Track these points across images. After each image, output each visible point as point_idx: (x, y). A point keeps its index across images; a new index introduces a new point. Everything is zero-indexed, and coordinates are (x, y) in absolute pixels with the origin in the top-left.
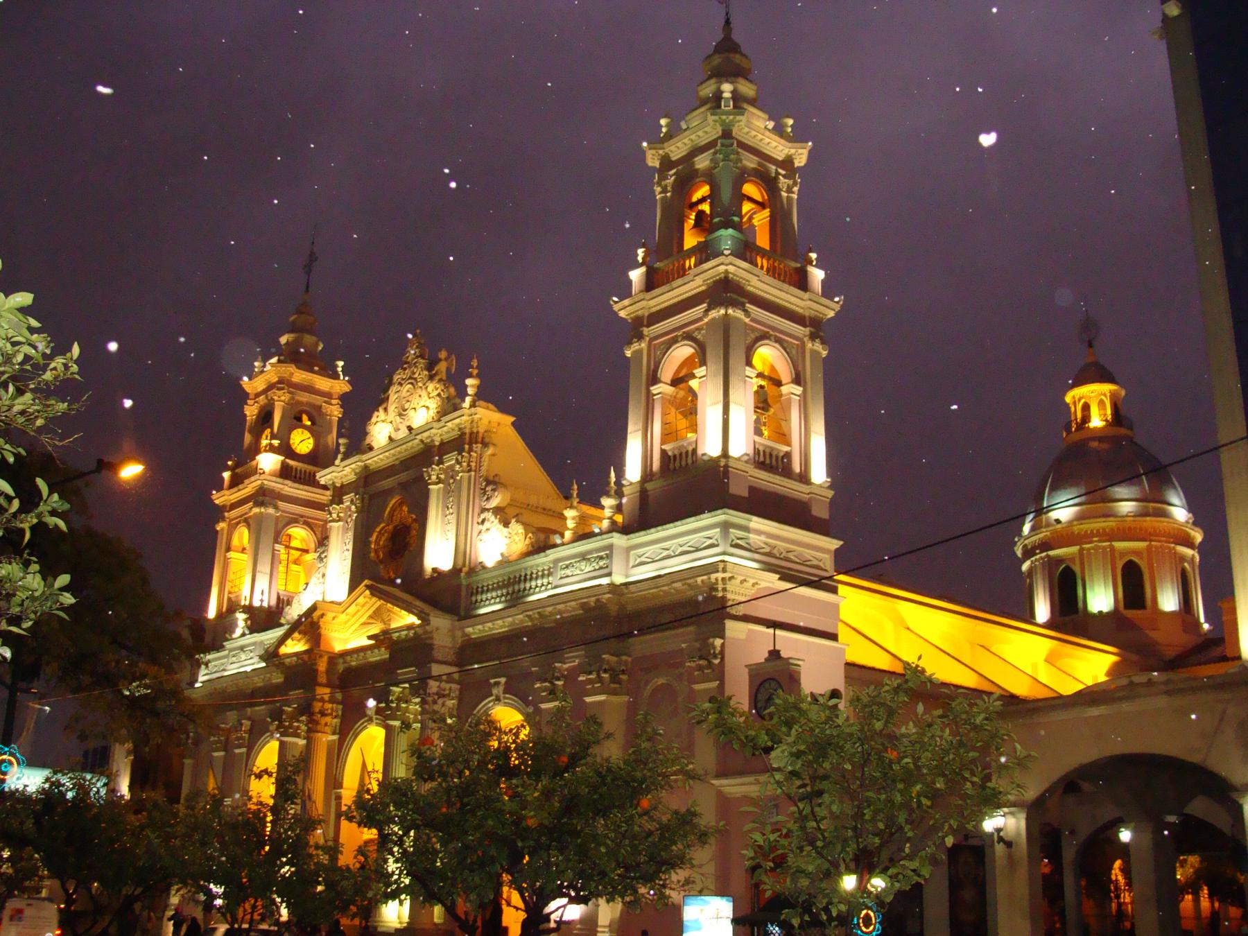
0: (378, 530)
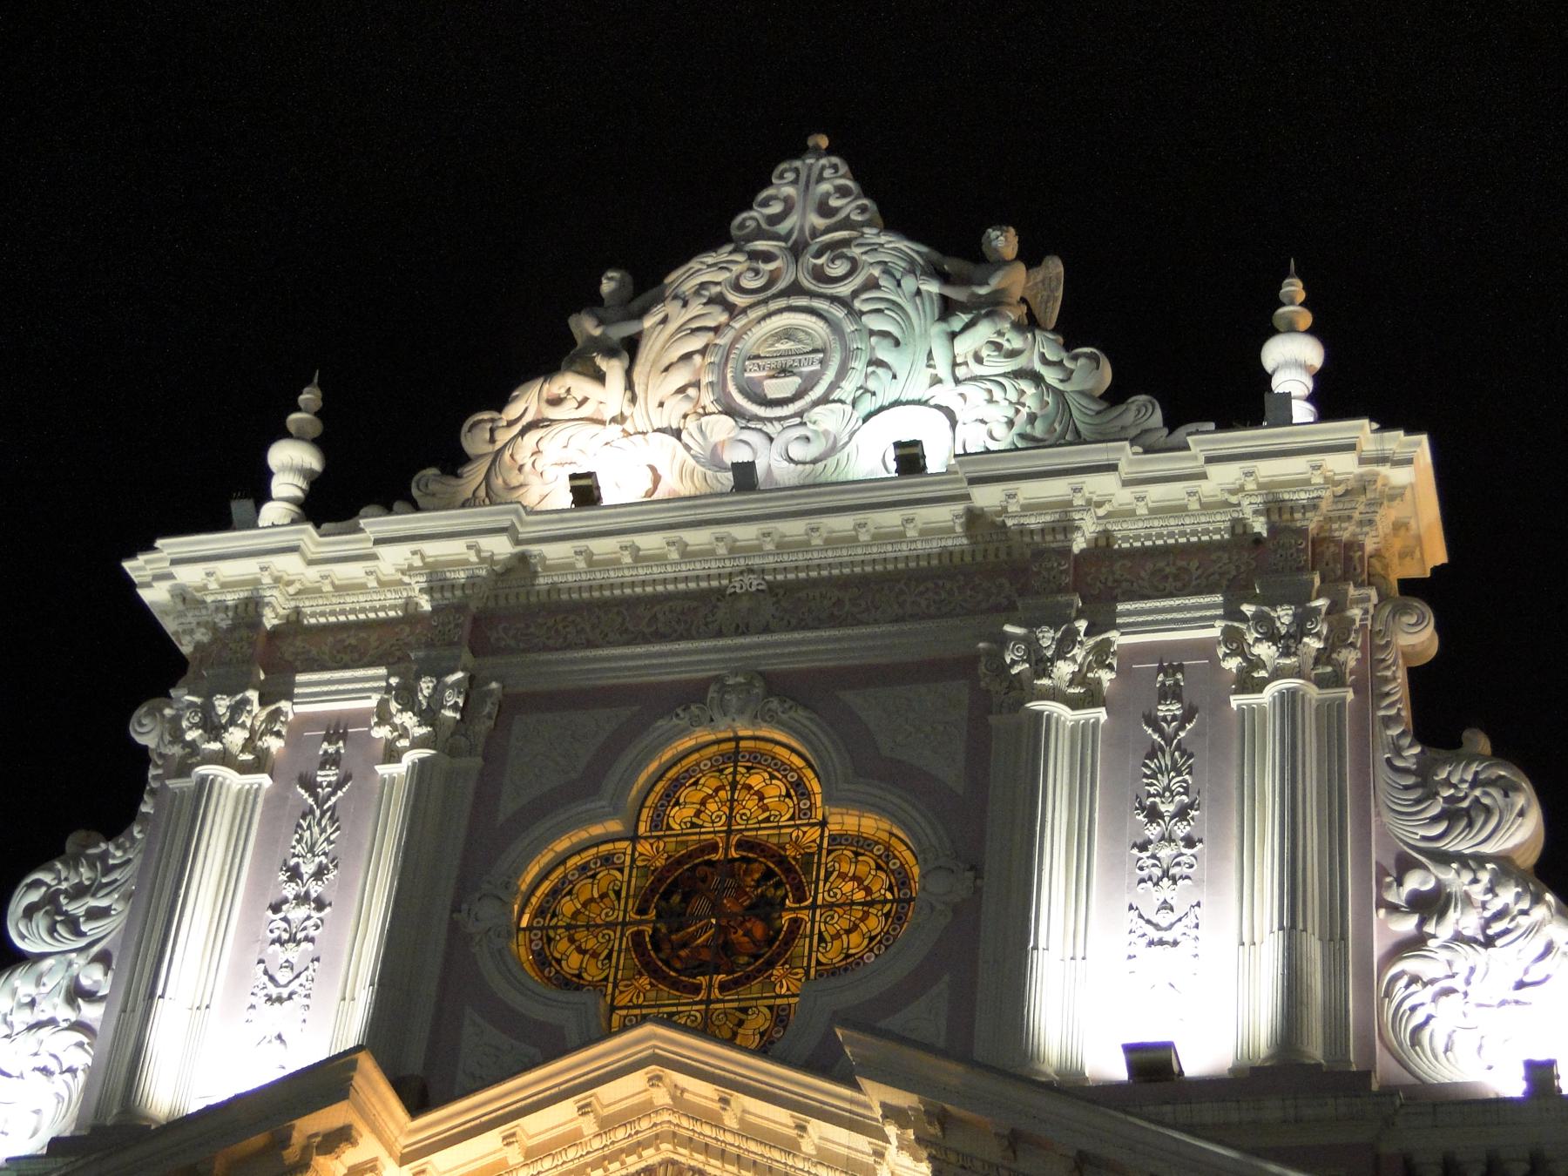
0: (562, 845)
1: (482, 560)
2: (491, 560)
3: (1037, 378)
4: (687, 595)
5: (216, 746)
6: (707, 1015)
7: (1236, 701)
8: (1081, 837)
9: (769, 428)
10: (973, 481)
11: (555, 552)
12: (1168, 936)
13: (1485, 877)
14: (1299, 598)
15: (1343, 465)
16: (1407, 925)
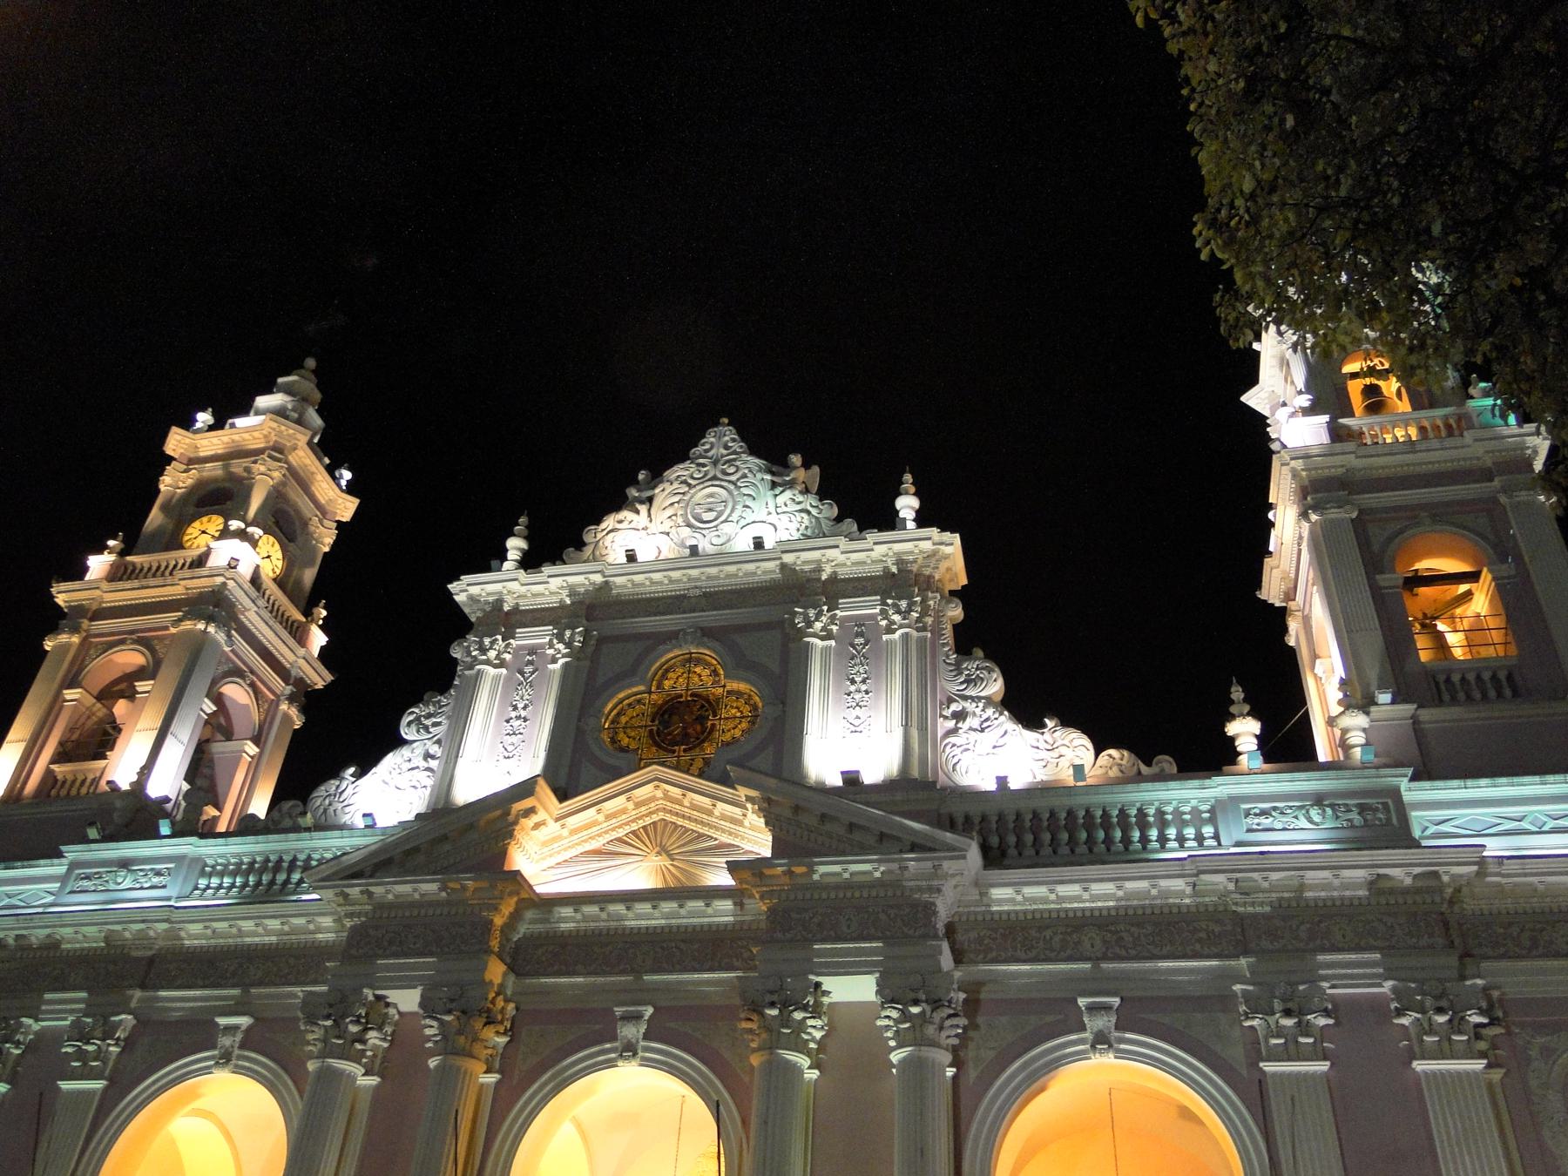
0: (621, 695)
1: (591, 584)
2: (594, 584)
3: (809, 513)
4: (671, 597)
5: (484, 657)
6: (678, 762)
7: (885, 637)
8: (825, 690)
9: (704, 532)
10: (783, 552)
11: (619, 580)
12: (858, 729)
13: (981, 705)
14: (910, 597)
15: (926, 546)
16: (951, 724)
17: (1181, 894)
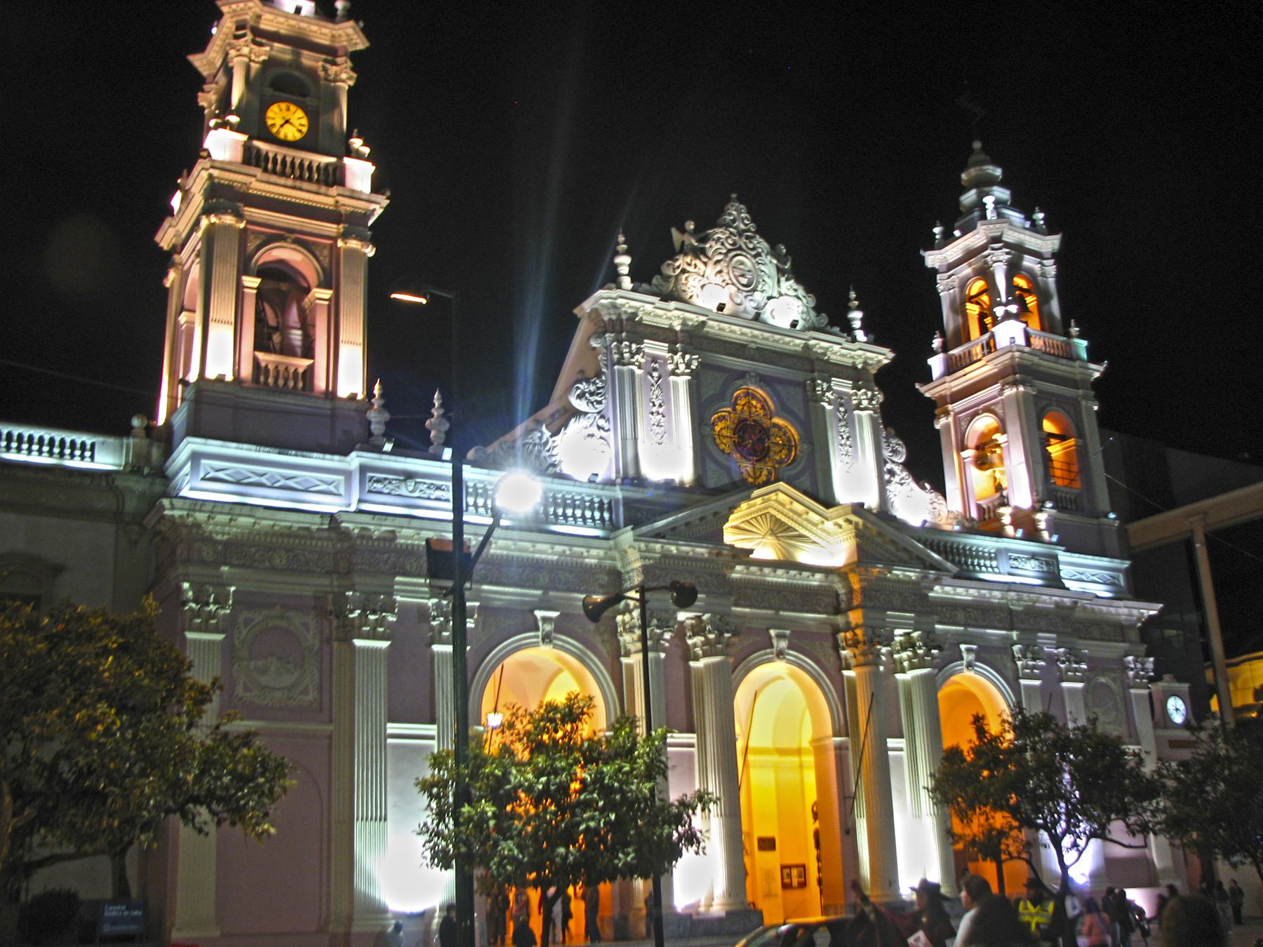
17: (995, 598)
